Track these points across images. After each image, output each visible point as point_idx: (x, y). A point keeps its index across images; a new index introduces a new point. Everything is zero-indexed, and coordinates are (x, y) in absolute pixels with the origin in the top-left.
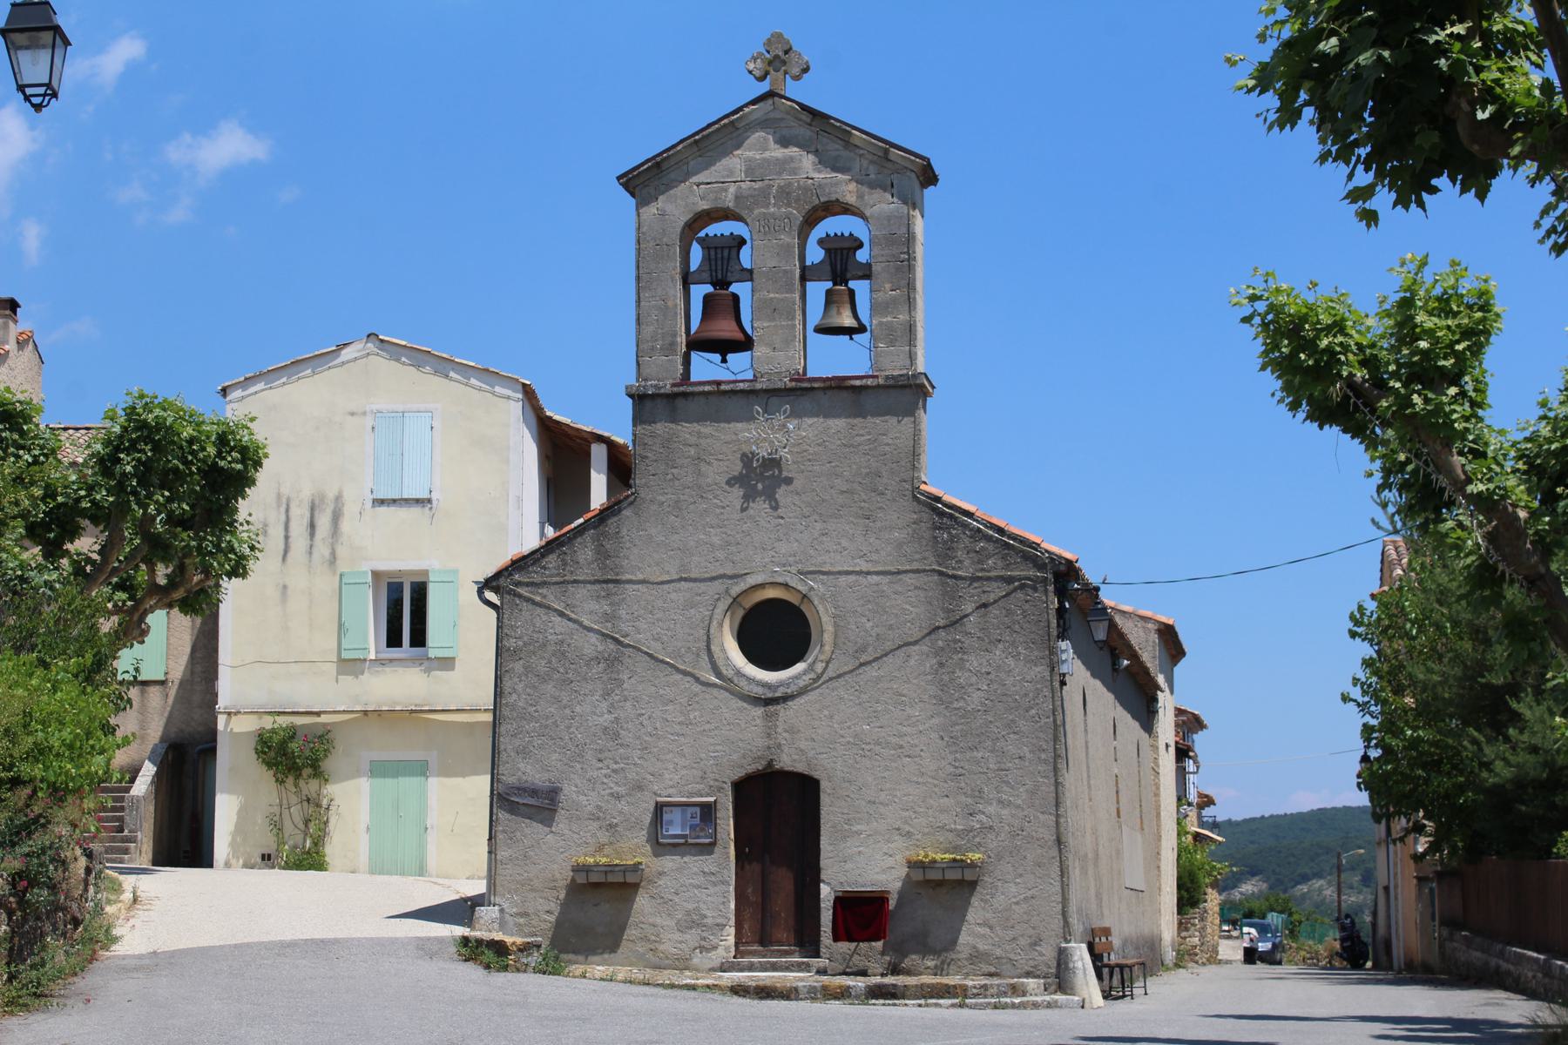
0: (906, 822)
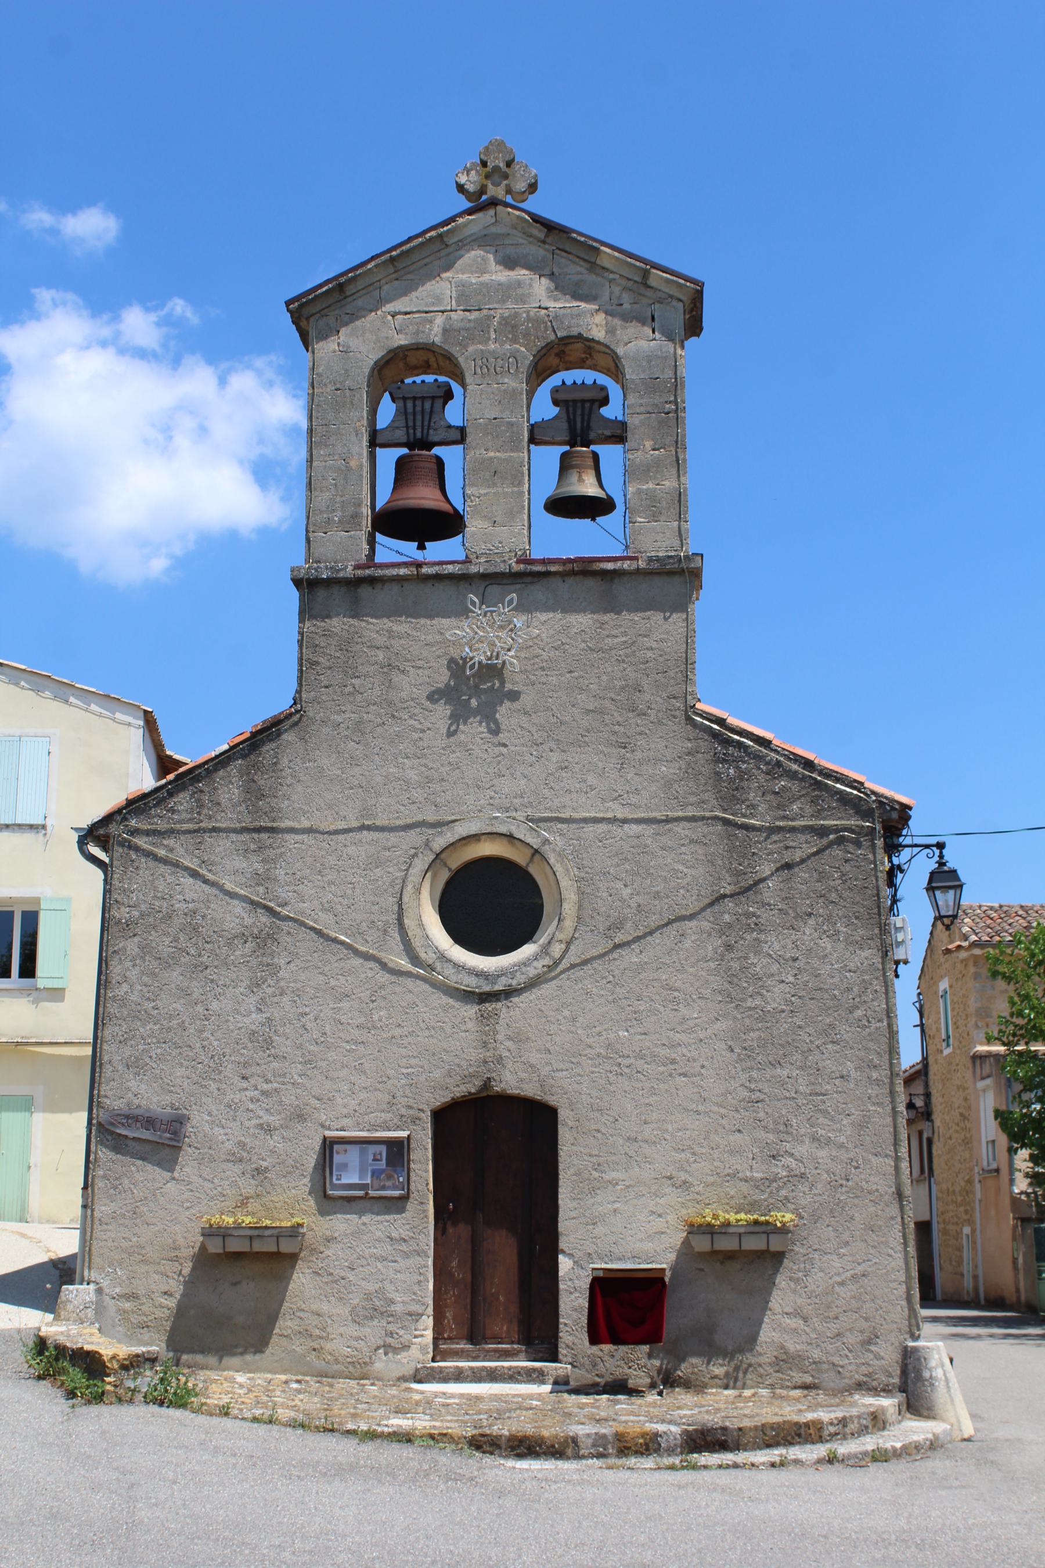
0: (681, 1169)
